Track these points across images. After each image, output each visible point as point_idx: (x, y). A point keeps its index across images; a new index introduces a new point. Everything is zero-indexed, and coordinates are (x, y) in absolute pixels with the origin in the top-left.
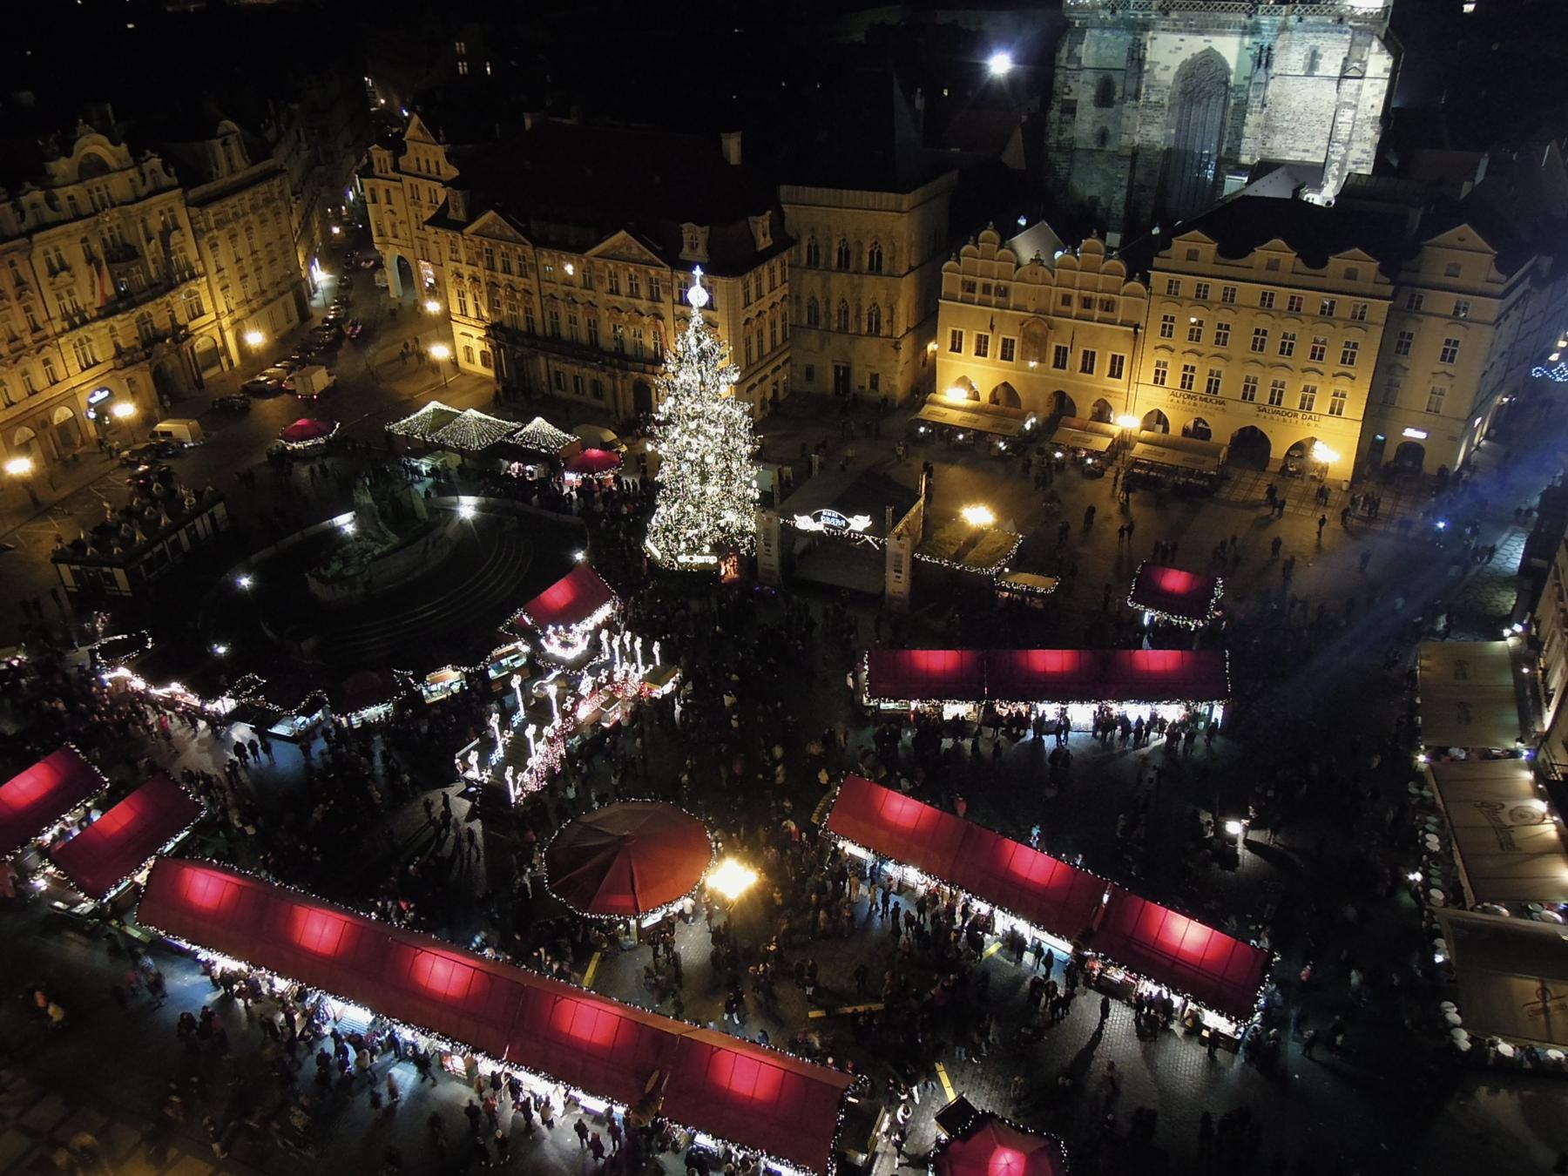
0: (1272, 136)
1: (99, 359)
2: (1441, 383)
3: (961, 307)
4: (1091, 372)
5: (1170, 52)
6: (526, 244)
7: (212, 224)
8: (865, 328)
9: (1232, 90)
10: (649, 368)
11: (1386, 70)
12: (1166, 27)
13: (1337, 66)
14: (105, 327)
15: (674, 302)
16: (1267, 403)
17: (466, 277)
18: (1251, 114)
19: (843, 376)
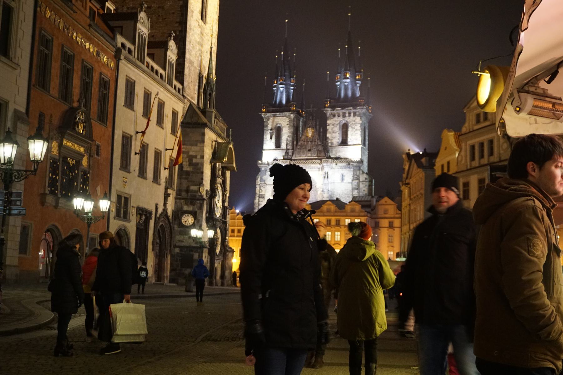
9: (318, 189)
18: (325, 194)
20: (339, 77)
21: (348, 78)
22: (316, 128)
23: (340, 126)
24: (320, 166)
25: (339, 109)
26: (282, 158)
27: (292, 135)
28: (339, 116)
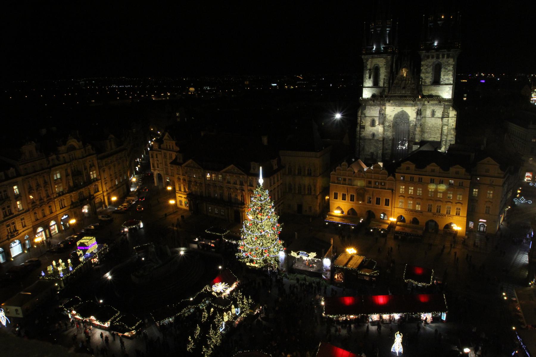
0: (424, 134)
1: (66, 205)
3: (337, 186)
4: (379, 204)
5: (391, 111)
6: (201, 169)
7: (104, 165)
8: (307, 192)
9: (411, 122)
10: (240, 206)
11: (455, 115)
12: (389, 105)
13: (441, 114)
14: (69, 196)
15: (248, 186)
16: (436, 212)
17: (181, 179)
19: (300, 207)
23: (433, 67)
28: (433, 57)
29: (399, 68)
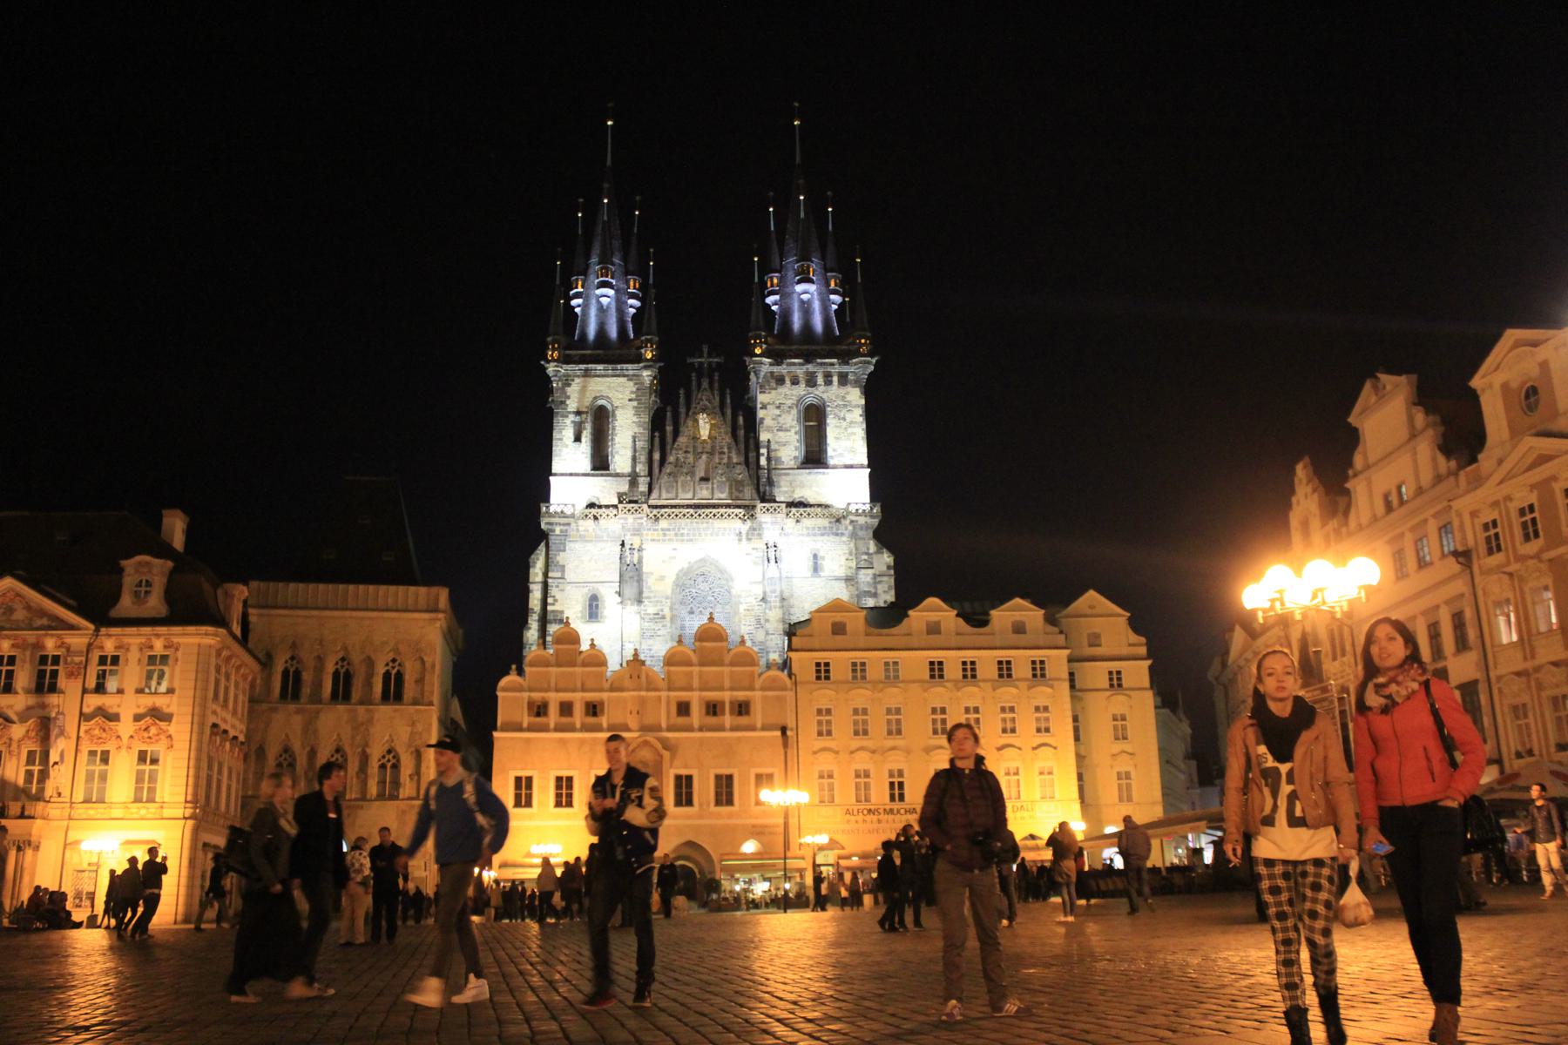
2: (1124, 765)
3: (528, 740)
5: (663, 562)
8: (373, 789)
9: (740, 596)
11: (889, 568)
13: (841, 566)
15: (85, 691)
18: (770, 609)
20: (775, 281)
21: (811, 281)
22: (723, 414)
23: (799, 412)
24: (745, 527)
25: (796, 361)
26: (615, 502)
27: (647, 433)
28: (795, 382)
29: (682, 410)
